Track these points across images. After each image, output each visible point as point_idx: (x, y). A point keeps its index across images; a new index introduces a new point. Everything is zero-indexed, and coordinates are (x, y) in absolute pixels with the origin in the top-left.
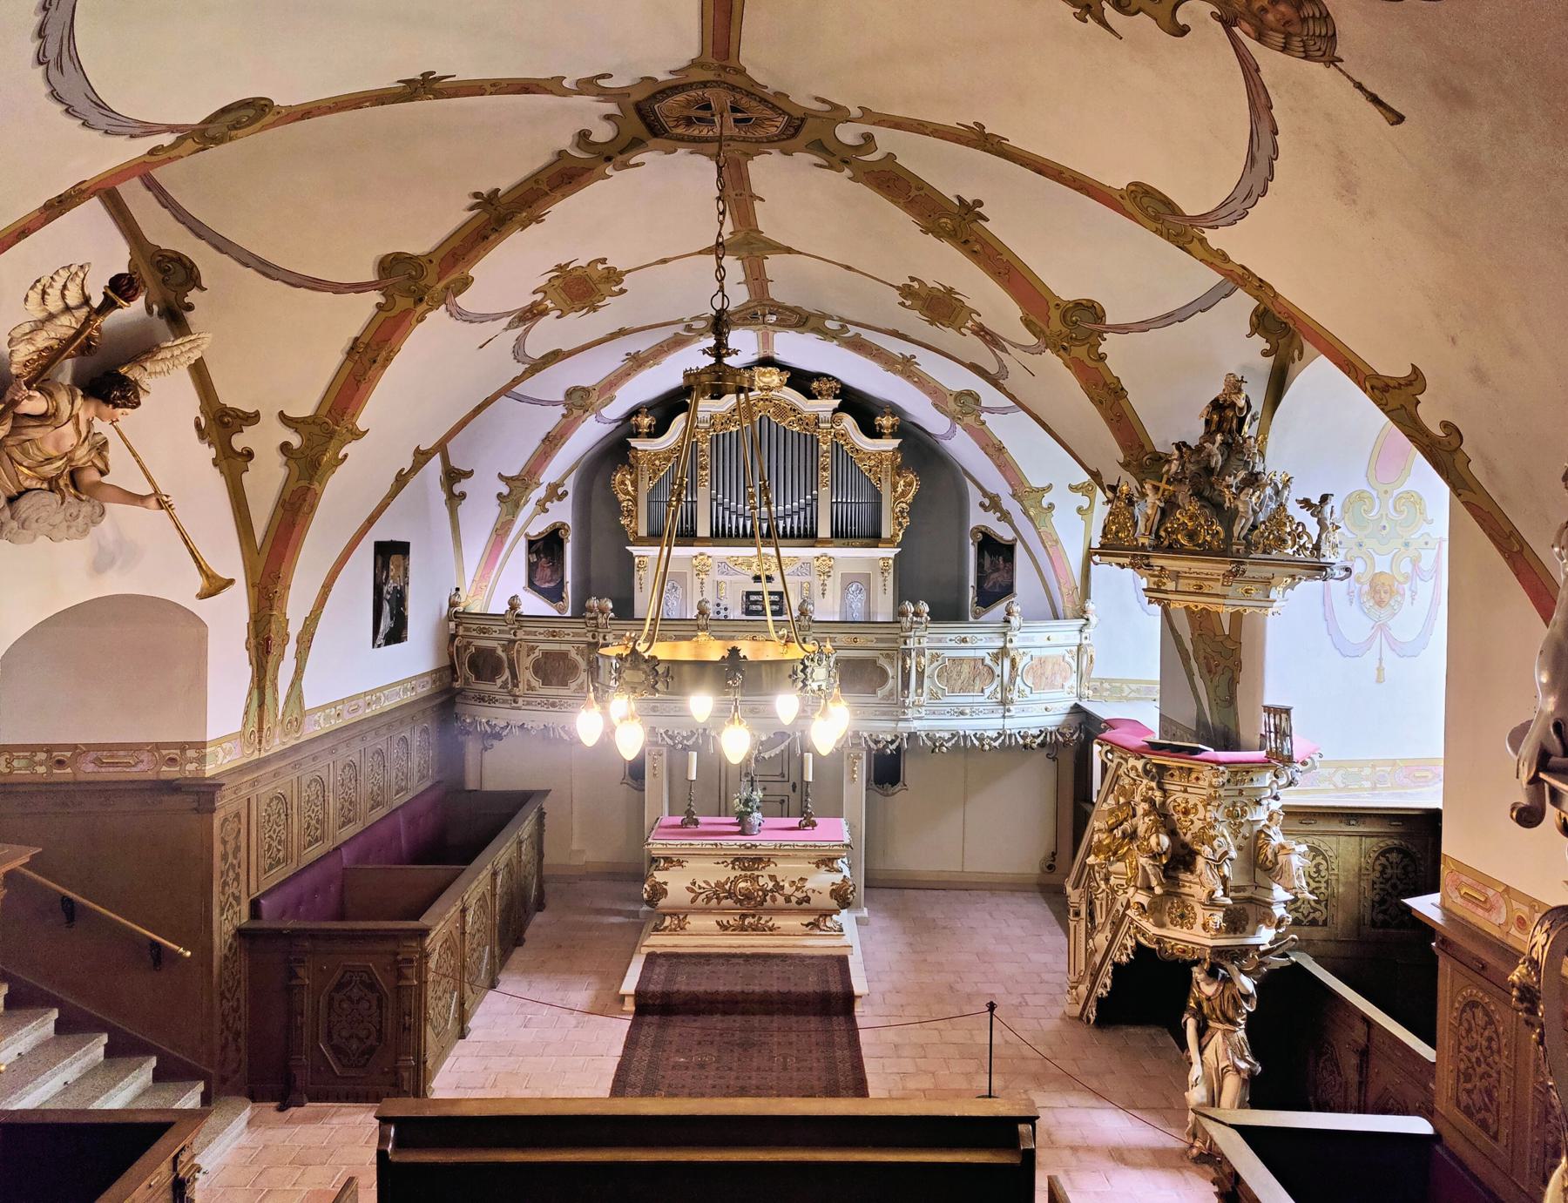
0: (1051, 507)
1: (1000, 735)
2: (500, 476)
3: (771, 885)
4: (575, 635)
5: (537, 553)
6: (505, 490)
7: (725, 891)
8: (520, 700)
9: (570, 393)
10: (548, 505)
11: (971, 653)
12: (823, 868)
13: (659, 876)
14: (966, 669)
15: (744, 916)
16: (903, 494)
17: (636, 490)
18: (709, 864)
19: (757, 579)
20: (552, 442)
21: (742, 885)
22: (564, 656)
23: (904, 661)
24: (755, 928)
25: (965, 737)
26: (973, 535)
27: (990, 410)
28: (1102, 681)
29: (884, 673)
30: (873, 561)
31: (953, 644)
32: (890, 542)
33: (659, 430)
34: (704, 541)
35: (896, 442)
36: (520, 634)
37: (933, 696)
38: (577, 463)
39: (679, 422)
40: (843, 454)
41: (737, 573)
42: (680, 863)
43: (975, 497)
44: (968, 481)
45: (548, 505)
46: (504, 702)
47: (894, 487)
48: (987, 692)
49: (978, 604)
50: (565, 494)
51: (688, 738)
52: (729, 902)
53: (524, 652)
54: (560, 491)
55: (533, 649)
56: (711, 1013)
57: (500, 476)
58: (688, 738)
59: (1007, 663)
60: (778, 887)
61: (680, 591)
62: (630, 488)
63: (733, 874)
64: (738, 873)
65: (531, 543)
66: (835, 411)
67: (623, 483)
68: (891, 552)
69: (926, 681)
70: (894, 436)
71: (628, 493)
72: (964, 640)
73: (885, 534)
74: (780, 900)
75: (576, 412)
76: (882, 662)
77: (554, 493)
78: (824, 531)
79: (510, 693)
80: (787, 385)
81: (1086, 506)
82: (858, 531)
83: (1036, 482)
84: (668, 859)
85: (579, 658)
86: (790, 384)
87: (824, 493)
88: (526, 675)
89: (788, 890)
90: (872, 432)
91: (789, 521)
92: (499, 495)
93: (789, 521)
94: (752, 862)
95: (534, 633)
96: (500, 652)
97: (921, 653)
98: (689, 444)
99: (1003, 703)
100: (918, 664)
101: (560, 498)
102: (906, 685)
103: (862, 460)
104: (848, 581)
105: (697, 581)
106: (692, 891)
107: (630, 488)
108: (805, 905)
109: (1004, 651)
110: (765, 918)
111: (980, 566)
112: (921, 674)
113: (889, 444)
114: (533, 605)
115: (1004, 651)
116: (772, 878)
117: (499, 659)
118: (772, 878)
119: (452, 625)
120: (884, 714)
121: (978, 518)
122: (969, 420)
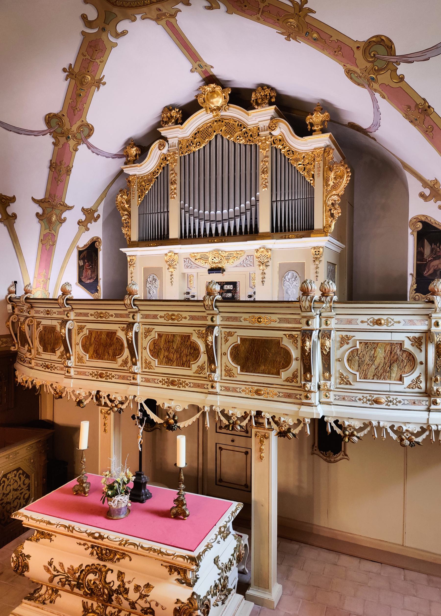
1: (423, 430)
6: (40, 211)
10: (89, 225)
11: (387, 337)
16: (335, 187)
19: (212, 270)
23: (304, 342)
25: (379, 428)
27: (408, 59)
30: (305, 251)
31: (365, 326)
32: (323, 232)
34: (174, 242)
35: (327, 135)
37: (343, 380)
40: (282, 160)
41: (198, 266)
45: (89, 225)
47: (326, 181)
48: (408, 380)
49: (417, 290)
50: (99, 216)
51: (122, 403)
61: (158, 282)
62: (127, 206)
69: (335, 366)
70: (323, 131)
71: (125, 210)
72: (378, 322)
73: (318, 225)
75: (63, 140)
78: (264, 226)
82: (293, 224)
87: (264, 196)
90: (302, 130)
91: (238, 220)
93: (238, 220)
97: (325, 334)
98: (164, 168)
99: (428, 393)
100: (323, 346)
101: (96, 220)
102: (307, 368)
103: (297, 160)
104: (285, 269)
107: (127, 206)
112: (326, 358)
113: (320, 141)
114: (79, 293)
116: (120, 574)
118: (120, 574)
119: (10, 307)
122: (384, 78)
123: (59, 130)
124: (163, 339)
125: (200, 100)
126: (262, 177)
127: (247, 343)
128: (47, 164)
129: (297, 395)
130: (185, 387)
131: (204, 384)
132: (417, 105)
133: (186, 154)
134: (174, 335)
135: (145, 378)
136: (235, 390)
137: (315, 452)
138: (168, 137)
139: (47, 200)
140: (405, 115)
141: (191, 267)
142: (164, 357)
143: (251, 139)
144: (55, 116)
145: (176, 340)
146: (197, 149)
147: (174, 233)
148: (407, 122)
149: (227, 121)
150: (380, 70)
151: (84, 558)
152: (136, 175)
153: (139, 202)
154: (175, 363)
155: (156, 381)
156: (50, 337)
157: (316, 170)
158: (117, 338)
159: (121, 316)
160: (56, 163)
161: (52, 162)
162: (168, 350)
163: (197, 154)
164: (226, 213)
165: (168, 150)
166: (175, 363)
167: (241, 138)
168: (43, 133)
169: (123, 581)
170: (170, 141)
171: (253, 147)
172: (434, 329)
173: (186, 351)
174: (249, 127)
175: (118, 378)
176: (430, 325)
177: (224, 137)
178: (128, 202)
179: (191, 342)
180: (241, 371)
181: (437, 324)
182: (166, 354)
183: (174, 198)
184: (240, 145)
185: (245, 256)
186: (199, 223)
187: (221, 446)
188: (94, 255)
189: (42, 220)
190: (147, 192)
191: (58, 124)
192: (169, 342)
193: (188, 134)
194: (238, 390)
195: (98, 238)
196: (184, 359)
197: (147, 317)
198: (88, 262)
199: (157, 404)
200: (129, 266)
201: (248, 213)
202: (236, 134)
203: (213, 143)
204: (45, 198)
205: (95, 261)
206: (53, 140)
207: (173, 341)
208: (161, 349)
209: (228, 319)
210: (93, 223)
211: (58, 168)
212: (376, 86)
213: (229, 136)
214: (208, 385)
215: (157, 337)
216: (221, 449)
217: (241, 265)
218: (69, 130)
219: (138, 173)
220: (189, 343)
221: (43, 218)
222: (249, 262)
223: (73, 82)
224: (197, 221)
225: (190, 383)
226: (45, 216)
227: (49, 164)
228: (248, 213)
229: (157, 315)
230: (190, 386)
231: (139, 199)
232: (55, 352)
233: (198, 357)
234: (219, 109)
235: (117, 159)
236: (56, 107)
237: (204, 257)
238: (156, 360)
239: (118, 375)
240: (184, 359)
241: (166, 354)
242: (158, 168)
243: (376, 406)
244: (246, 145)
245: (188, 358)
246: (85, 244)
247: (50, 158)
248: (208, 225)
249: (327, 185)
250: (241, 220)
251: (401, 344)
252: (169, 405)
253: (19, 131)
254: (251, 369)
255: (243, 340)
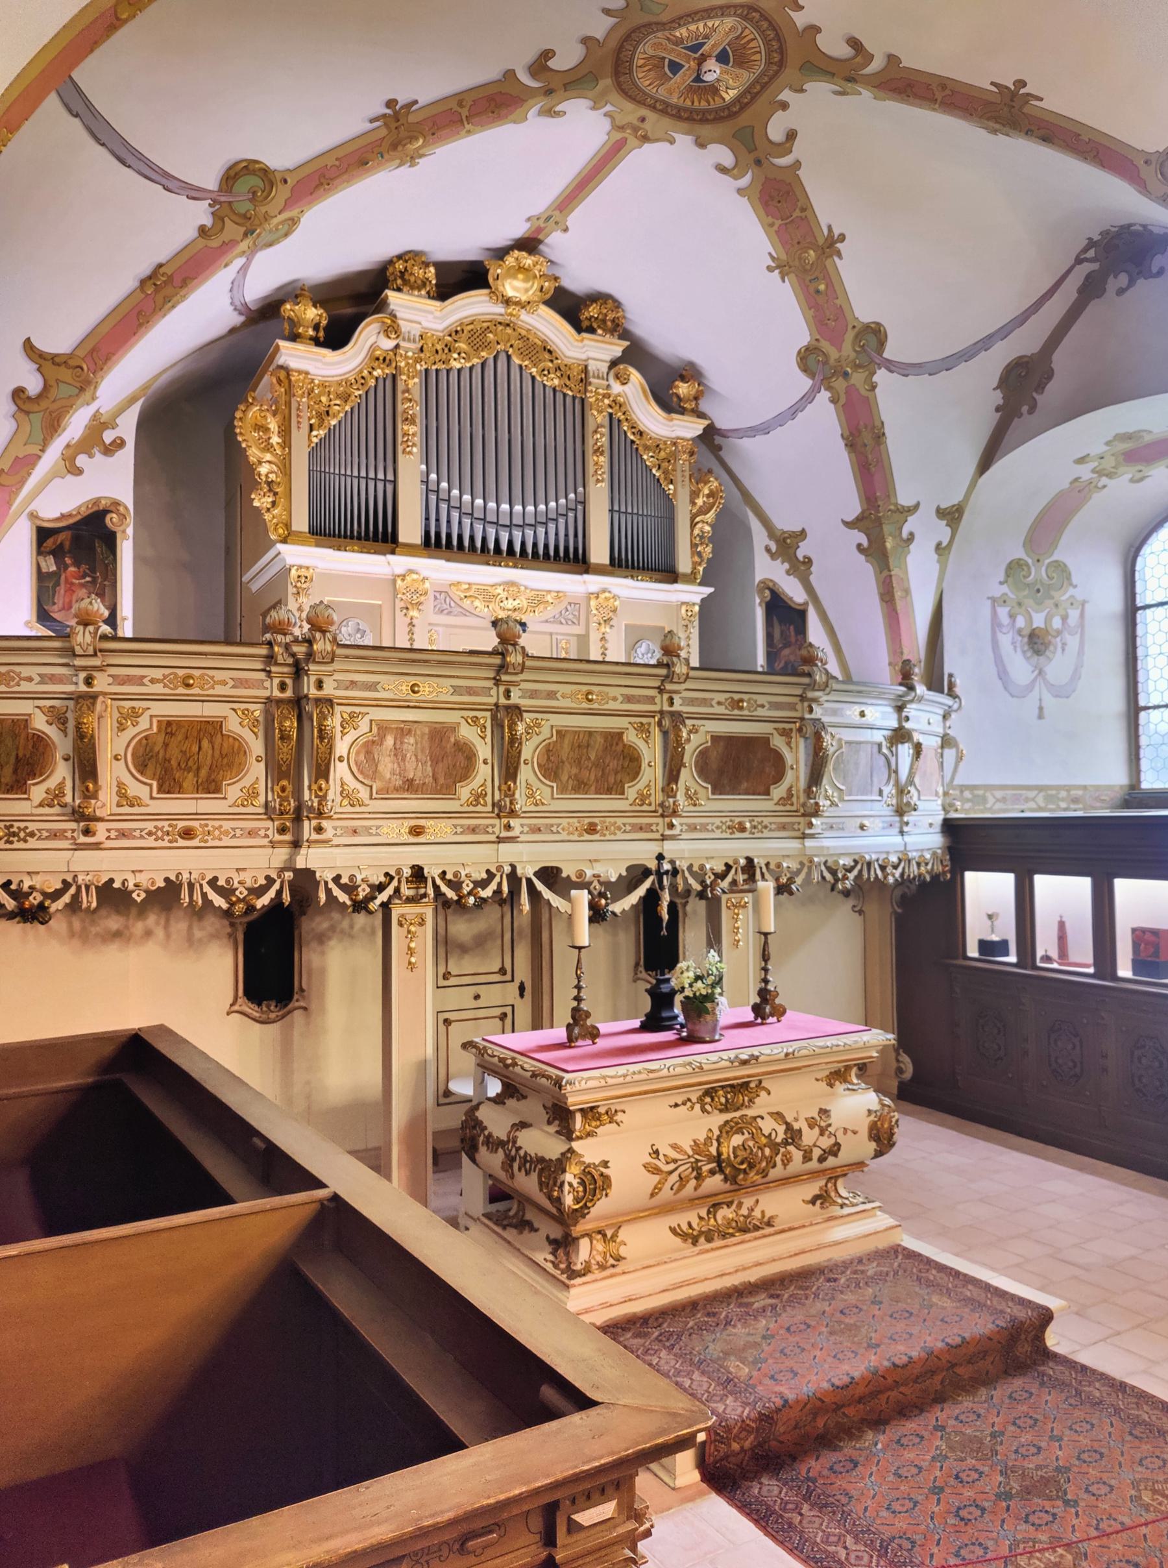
0: (912, 535)
2: (29, 347)
3: (781, 1129)
4: (239, 683)
5: (57, 553)
6: (33, 384)
7: (711, 1158)
8: (101, 829)
9: (240, 173)
10: (81, 460)
12: (840, 1087)
13: (589, 1151)
14: (864, 757)
15: (716, 1206)
17: (287, 443)
18: (659, 1108)
20: (162, 287)
21: (737, 1140)
22: (211, 729)
24: (745, 1228)
26: (760, 592)
27: (891, 366)
28: (962, 788)
29: (779, 759)
30: (666, 606)
32: (690, 579)
33: (336, 336)
36: (102, 683)
38: (145, 387)
39: (369, 336)
41: (465, 613)
42: (611, 1116)
43: (760, 538)
44: (751, 515)
45: (81, 460)
46: (55, 835)
52: (715, 1182)
53: (109, 724)
54: (108, 437)
55: (135, 714)
56: (850, 1431)
57: (29, 347)
58: (483, 884)
59: (905, 750)
60: (793, 1136)
62: (275, 440)
63: (717, 1120)
64: (717, 1120)
65: (43, 534)
66: (614, 364)
67: (262, 428)
68: (693, 594)
71: (268, 448)
74: (797, 1155)
75: (232, 230)
76: (778, 742)
77: (96, 440)
78: (599, 553)
79: (78, 815)
80: (547, 303)
81: (944, 544)
83: (904, 498)
84: (590, 1112)
85: (246, 734)
86: (550, 303)
88: (113, 772)
89: (809, 1136)
91: (541, 531)
92: (18, 394)
93: (541, 531)
94: (732, 1093)
95: (139, 681)
96: (40, 723)
101: (110, 449)
103: (647, 448)
105: (402, 622)
106: (656, 1171)
108: (831, 1161)
109: (900, 735)
110: (748, 1202)
111: (769, 637)
113: (688, 428)
115: (900, 735)
116: (778, 1116)
117: (40, 743)
118: (778, 1116)
120: (783, 827)
121: (768, 569)
122: (857, 378)
123: (244, 207)
124: (566, 741)
125: (495, 270)
126: (591, 459)
127: (722, 744)
128: (144, 268)
129: (794, 824)
130: (615, 834)
131: (651, 825)
132: (874, 427)
133: (434, 367)
134: (590, 733)
135: (529, 825)
136: (704, 828)
137: (640, 975)
138: (398, 315)
139: (72, 363)
140: (847, 433)
141: (449, 613)
142: (570, 777)
143: (568, 383)
144: (265, 173)
145: (595, 742)
146: (458, 366)
147: (410, 530)
148: (841, 443)
149: (524, 333)
150: (860, 366)
151: (697, 1127)
152: (307, 373)
153: (315, 440)
154: (593, 788)
155: (554, 829)
156: (195, 748)
157: (679, 474)
158: (456, 744)
159: (470, 691)
160: (170, 279)
161: (162, 270)
162: (578, 762)
163: (465, 375)
164: (524, 513)
165: (397, 346)
166: (593, 788)
167: (552, 376)
168: (194, 193)
169: (787, 1124)
170: (404, 327)
171: (569, 401)
172: (907, 725)
173: (613, 764)
174: (567, 361)
175: (462, 833)
176: (900, 720)
177: (516, 360)
178: (286, 432)
179: (625, 745)
180: (713, 793)
181: (907, 719)
182: (574, 771)
183: (410, 453)
184: (545, 386)
185: (565, 604)
186: (460, 523)
187: (446, 1015)
188: (100, 548)
189: (27, 413)
190: (334, 422)
191: (254, 193)
192: (579, 746)
193: (441, 327)
194: (709, 827)
195: (117, 503)
196: (612, 780)
197: (533, 694)
198: (77, 564)
199: (564, 875)
200: (291, 590)
201: (562, 521)
202: (542, 365)
203: (491, 362)
204: (71, 356)
205: (107, 566)
206: (208, 221)
207: (588, 746)
208: (563, 762)
209: (691, 702)
210: (99, 457)
211: (168, 290)
212: (840, 384)
213: (526, 363)
214: (657, 824)
215: (554, 738)
216: (447, 1022)
217: (556, 620)
218: (267, 218)
219: (312, 370)
220: (619, 748)
221: (35, 408)
222: (571, 617)
223: (384, 132)
224: (455, 515)
225: (624, 825)
226: (44, 404)
227: (148, 272)
228: (562, 521)
229: (555, 693)
230: (625, 831)
231: (314, 433)
232: (218, 790)
233: (638, 773)
234: (523, 305)
235: (236, 313)
236: (281, 155)
237: (488, 596)
238: (555, 785)
239: (462, 826)
240: (612, 780)
241: (574, 771)
242: (365, 373)
243: (863, 833)
244: (554, 390)
245: (619, 777)
246: (65, 511)
247: (162, 258)
248: (479, 528)
249: (693, 503)
250: (546, 533)
251: (880, 745)
252: (595, 872)
253: (126, 155)
254: (728, 788)
255: (716, 739)
